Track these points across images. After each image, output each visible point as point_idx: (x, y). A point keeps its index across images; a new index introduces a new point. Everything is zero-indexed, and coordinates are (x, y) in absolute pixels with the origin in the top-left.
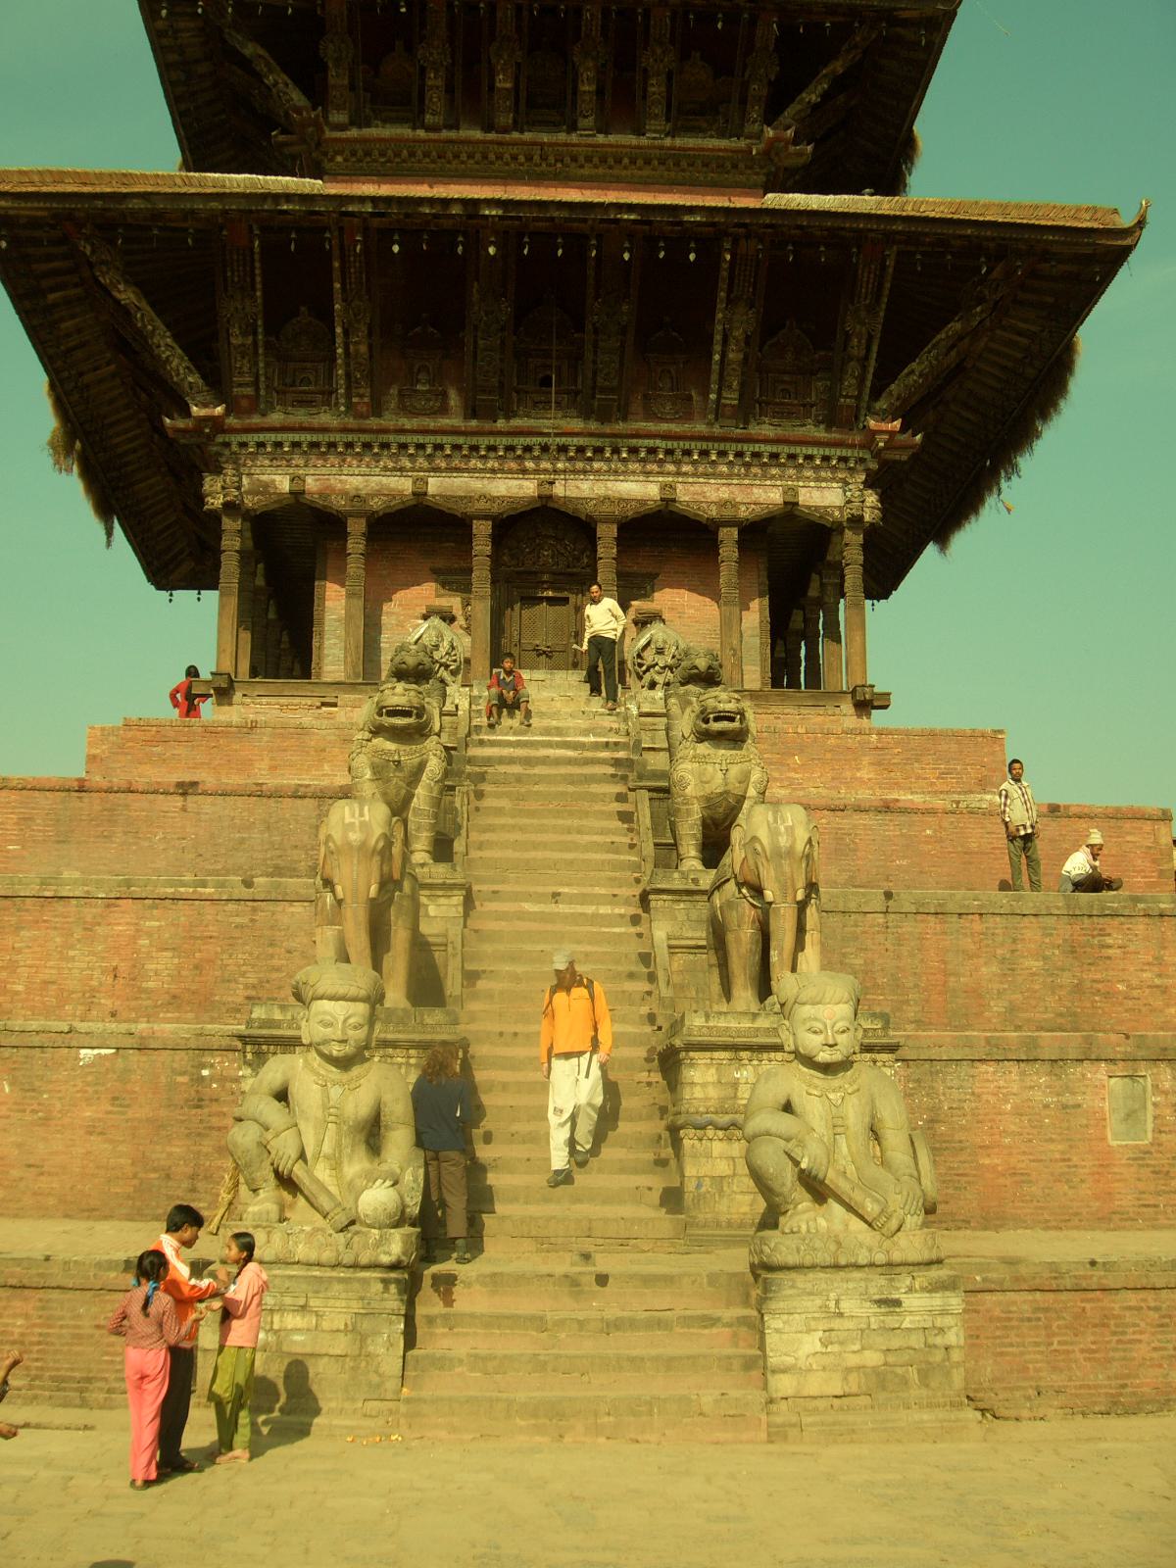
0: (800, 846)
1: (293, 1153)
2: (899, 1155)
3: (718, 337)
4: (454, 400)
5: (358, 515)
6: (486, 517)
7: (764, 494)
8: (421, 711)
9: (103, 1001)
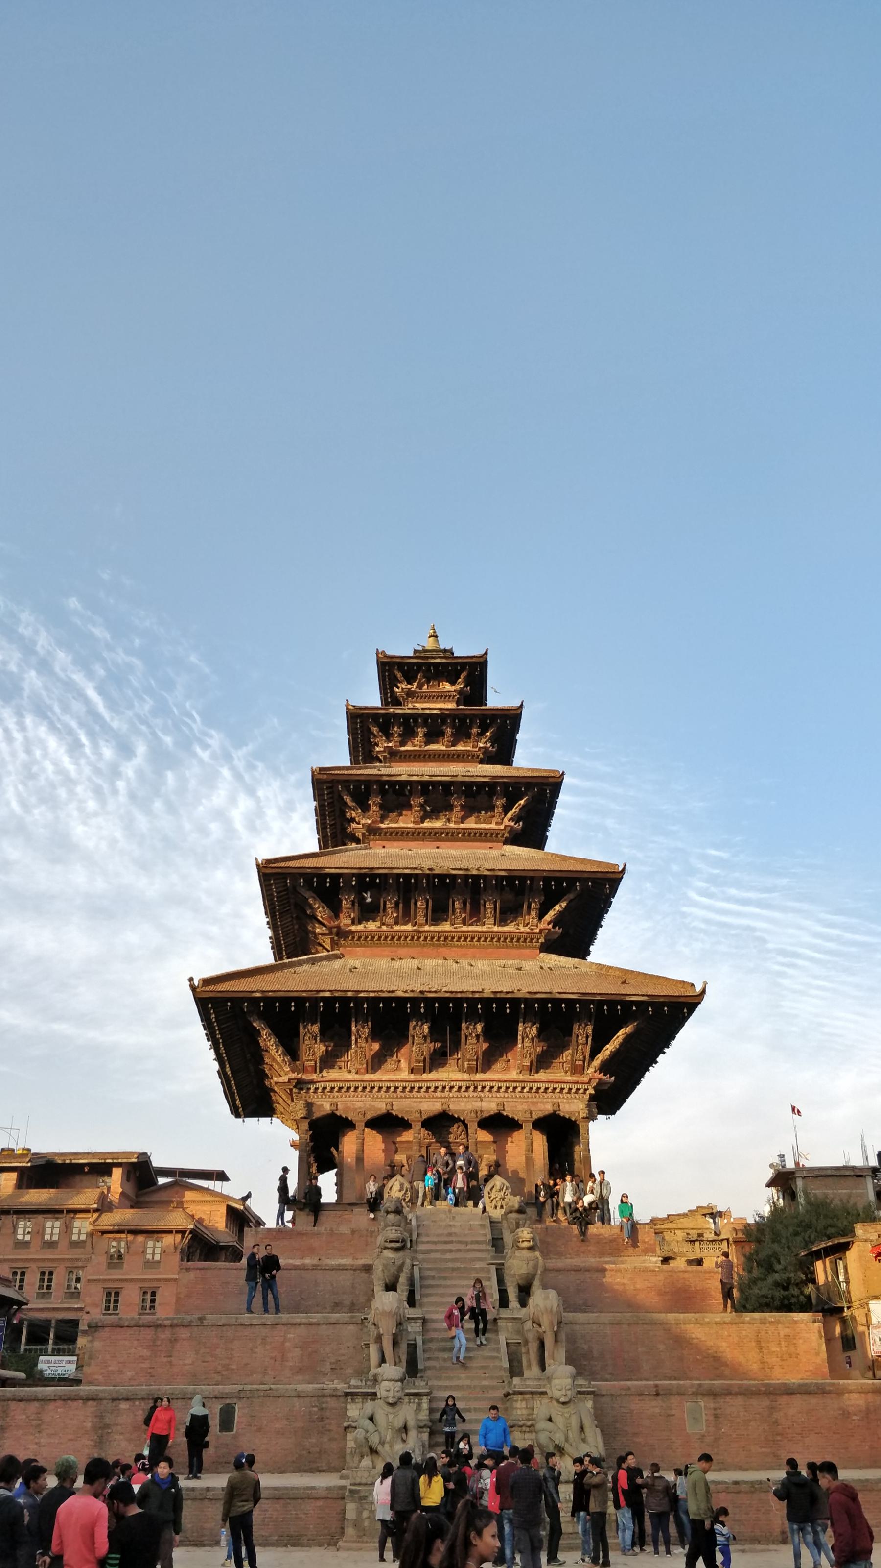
0: (555, 1308)
1: (377, 1440)
2: (590, 1439)
3: (519, 1037)
4: (404, 1064)
5: (361, 1121)
6: (419, 1121)
7: (545, 1107)
8: (404, 1240)
9: (270, 1372)
